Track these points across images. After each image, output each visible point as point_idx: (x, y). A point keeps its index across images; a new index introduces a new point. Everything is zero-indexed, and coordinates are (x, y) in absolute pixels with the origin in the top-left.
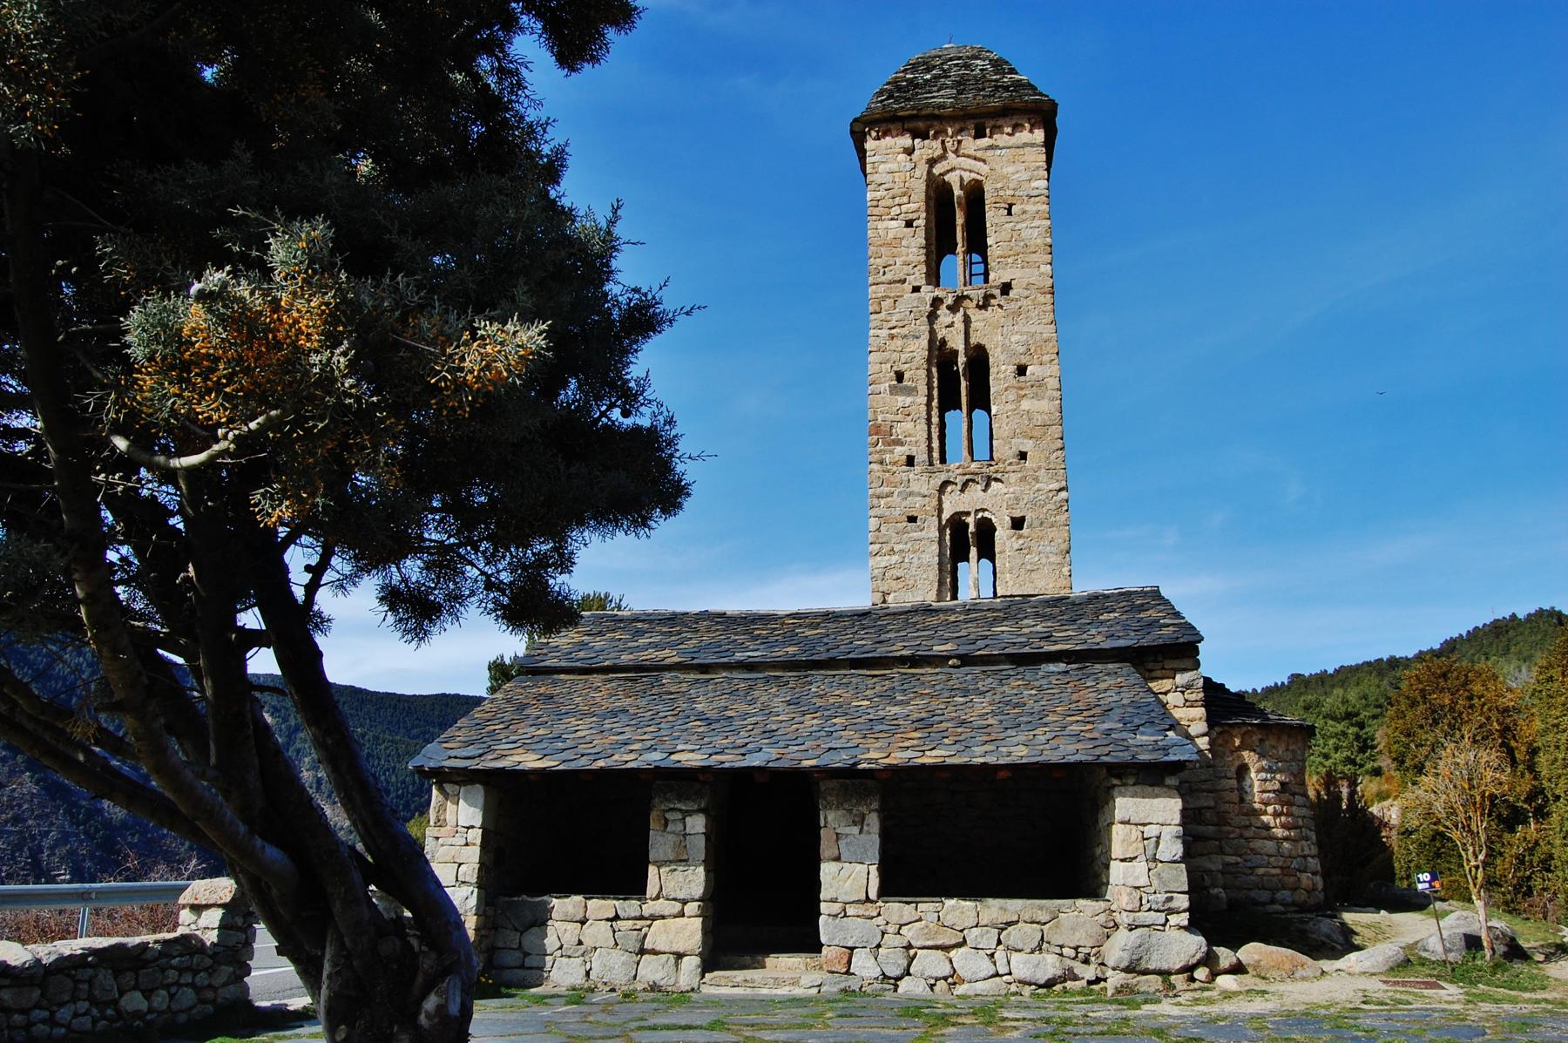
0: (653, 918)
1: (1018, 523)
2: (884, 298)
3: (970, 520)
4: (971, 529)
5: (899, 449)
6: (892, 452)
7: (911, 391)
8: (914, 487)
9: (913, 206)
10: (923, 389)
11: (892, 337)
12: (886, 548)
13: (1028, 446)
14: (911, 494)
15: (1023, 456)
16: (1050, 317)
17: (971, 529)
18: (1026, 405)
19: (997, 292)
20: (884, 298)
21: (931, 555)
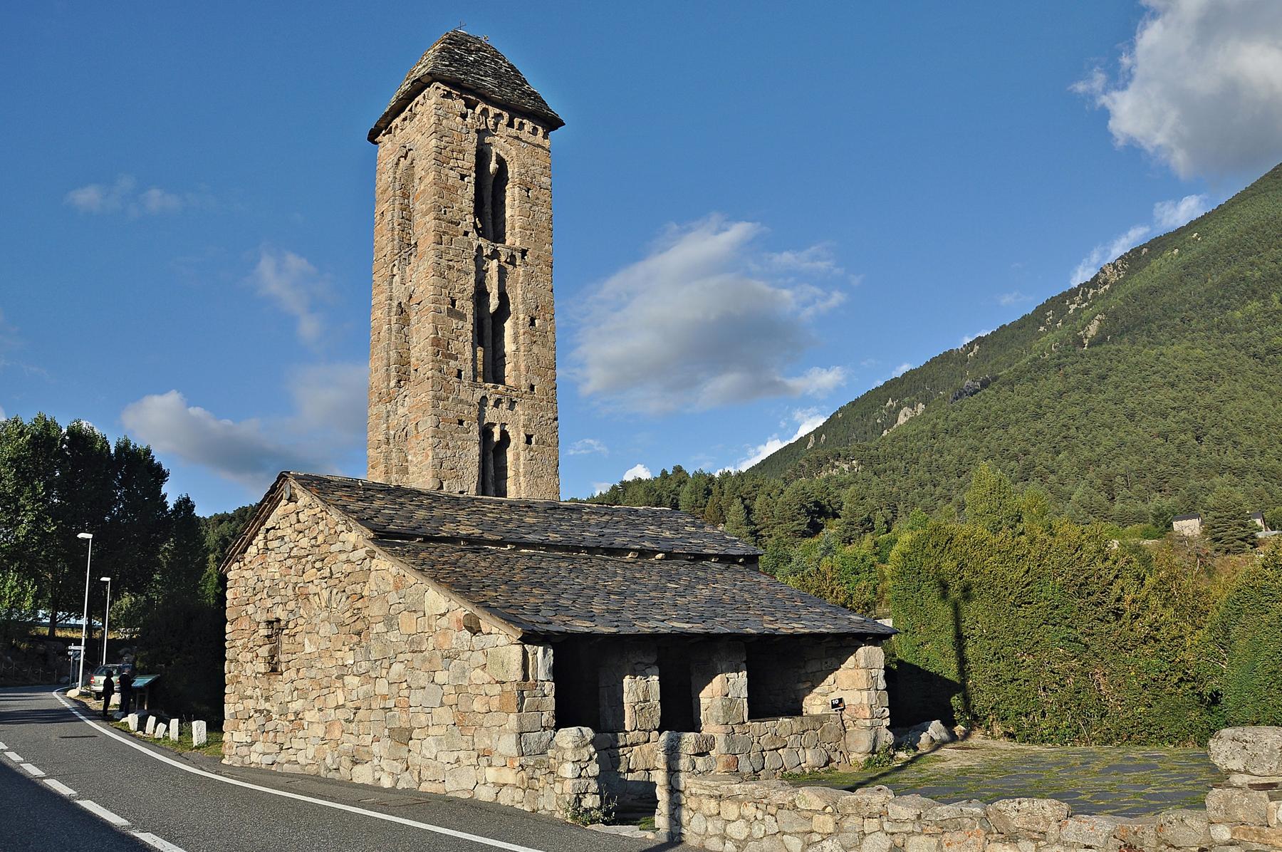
0: (632, 745)
1: (529, 439)
2: (444, 233)
3: (496, 431)
4: (497, 437)
5: (452, 363)
6: (448, 363)
7: (462, 317)
8: (463, 396)
9: (467, 165)
10: (470, 318)
11: (450, 268)
12: (443, 443)
13: (536, 381)
14: (461, 401)
15: (532, 388)
16: (549, 287)
17: (497, 437)
18: (535, 349)
19: (518, 255)
20: (444, 233)
21: (475, 451)
